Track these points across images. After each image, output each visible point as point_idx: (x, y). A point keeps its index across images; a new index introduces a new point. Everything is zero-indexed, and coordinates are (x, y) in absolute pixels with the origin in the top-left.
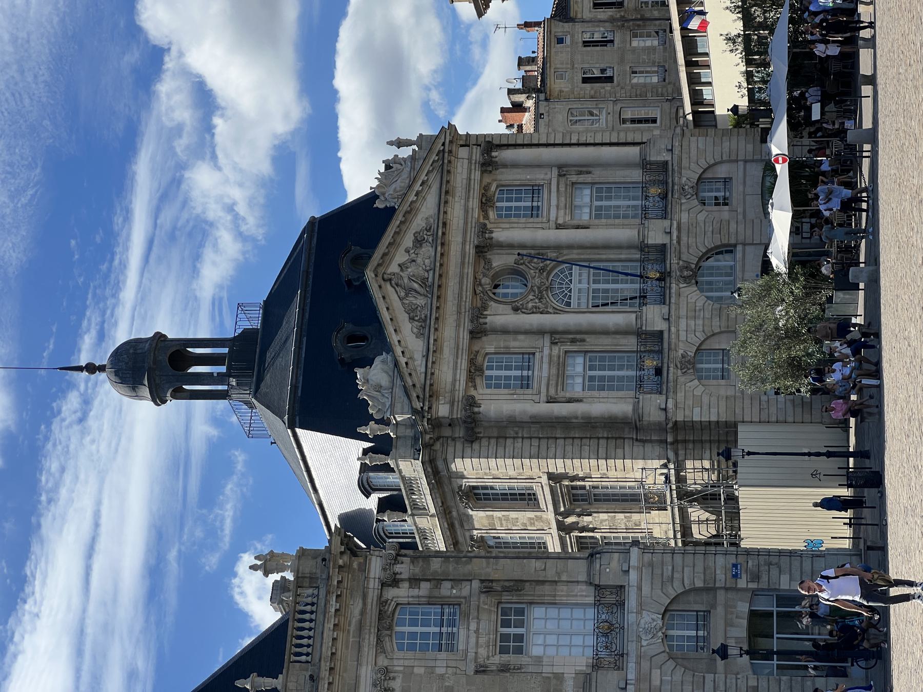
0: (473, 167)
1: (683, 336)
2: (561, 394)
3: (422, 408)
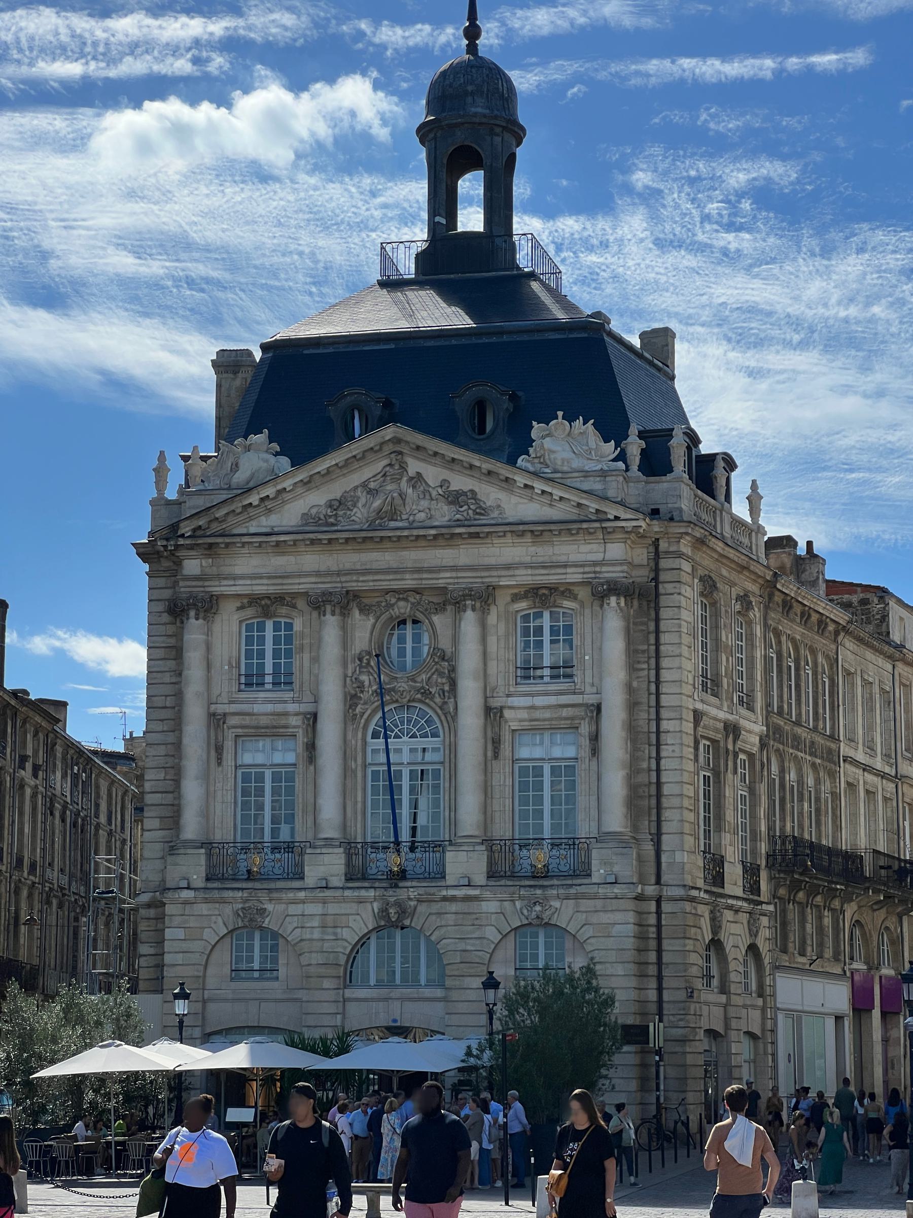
0: (587, 569)
1: (293, 909)
2: (230, 734)
3: (182, 536)
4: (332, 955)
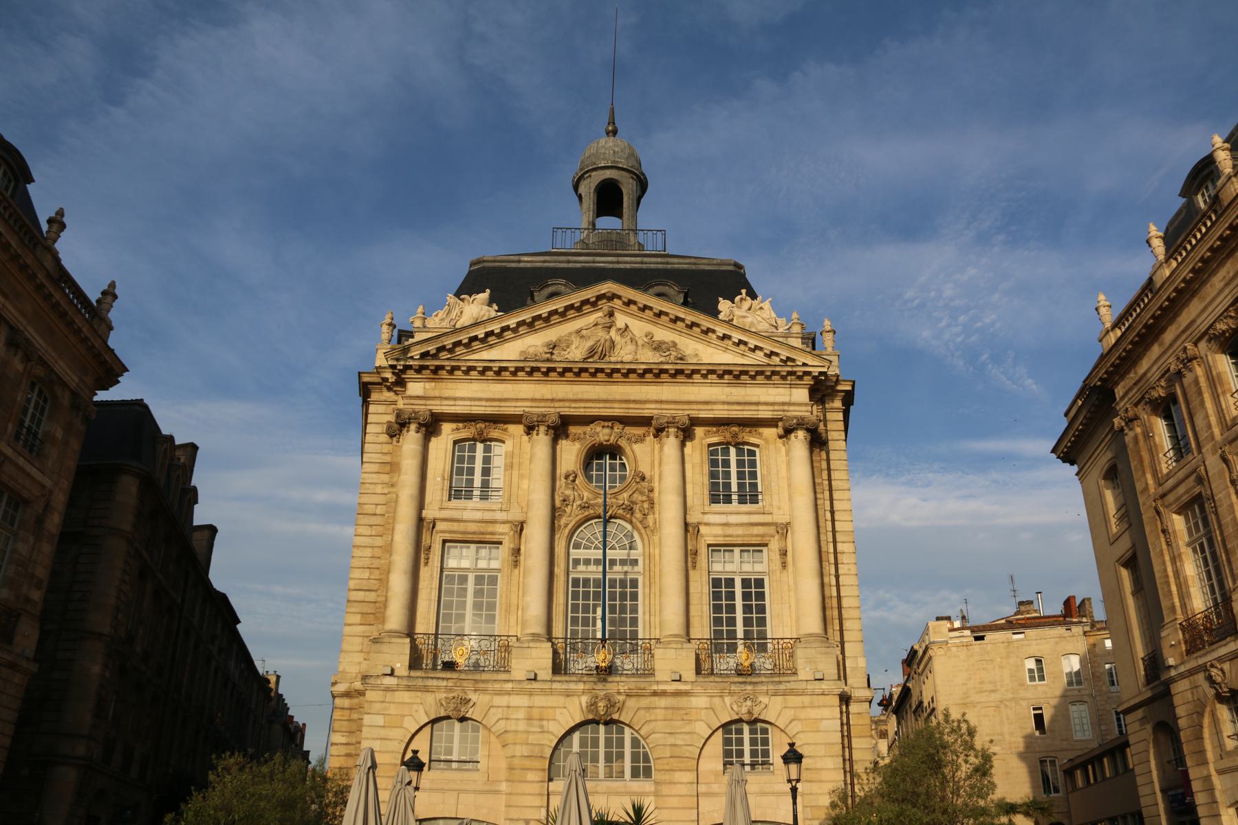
3: (412, 358)
4: (537, 749)
